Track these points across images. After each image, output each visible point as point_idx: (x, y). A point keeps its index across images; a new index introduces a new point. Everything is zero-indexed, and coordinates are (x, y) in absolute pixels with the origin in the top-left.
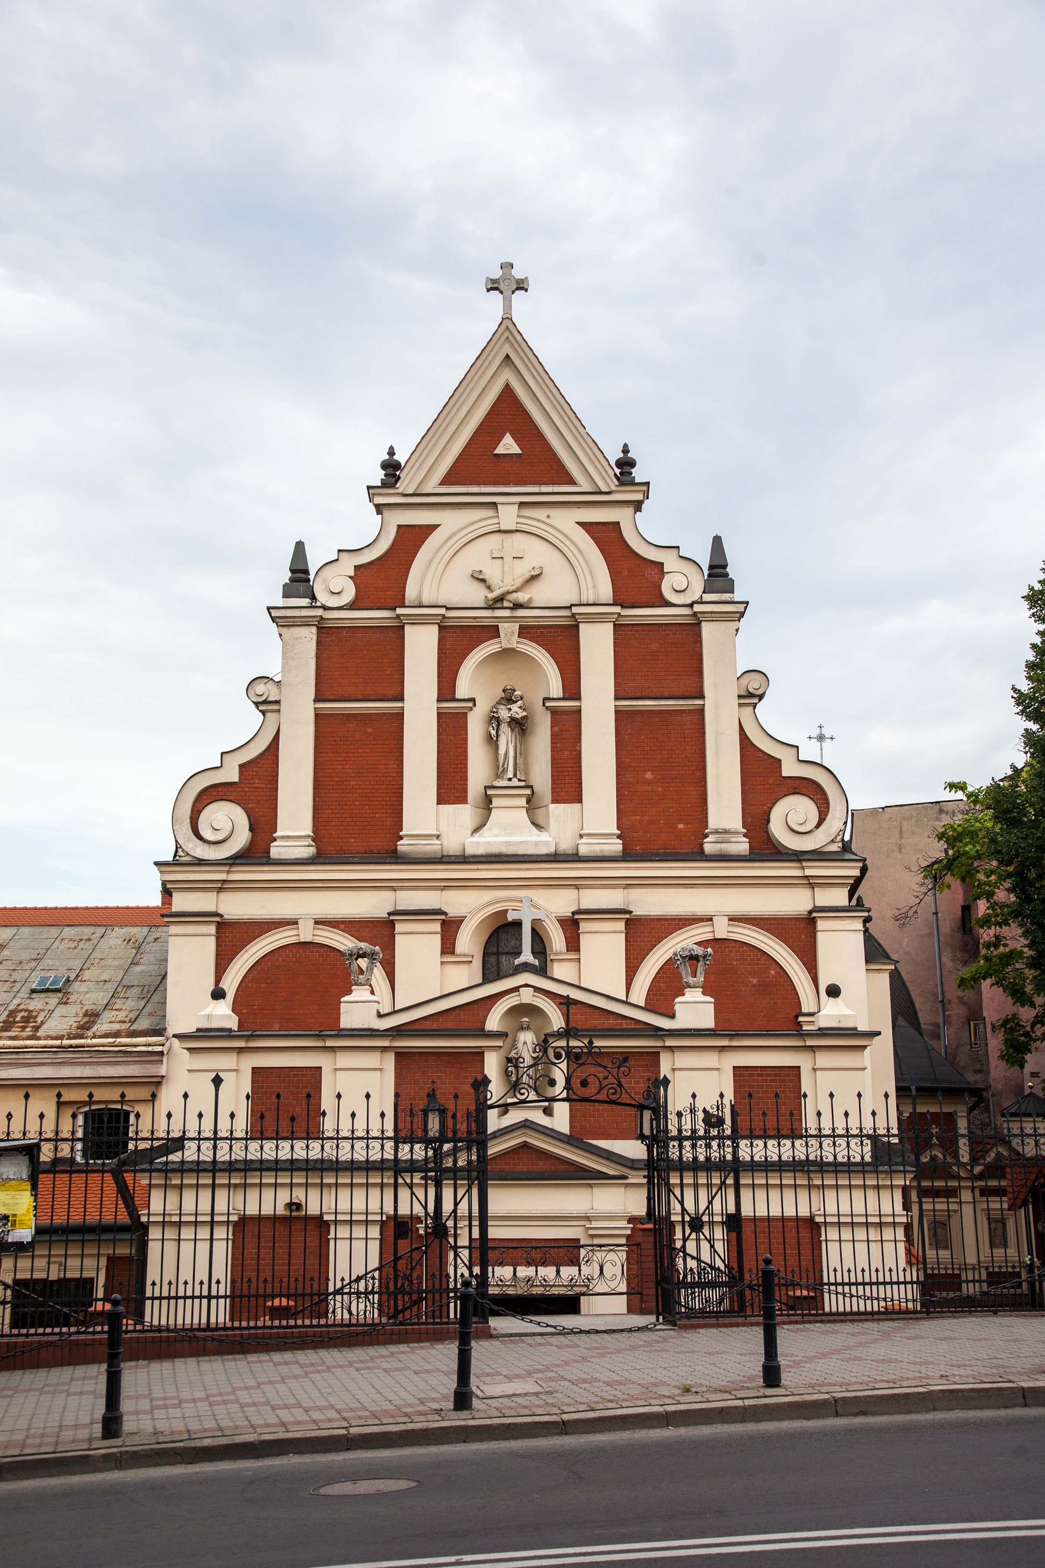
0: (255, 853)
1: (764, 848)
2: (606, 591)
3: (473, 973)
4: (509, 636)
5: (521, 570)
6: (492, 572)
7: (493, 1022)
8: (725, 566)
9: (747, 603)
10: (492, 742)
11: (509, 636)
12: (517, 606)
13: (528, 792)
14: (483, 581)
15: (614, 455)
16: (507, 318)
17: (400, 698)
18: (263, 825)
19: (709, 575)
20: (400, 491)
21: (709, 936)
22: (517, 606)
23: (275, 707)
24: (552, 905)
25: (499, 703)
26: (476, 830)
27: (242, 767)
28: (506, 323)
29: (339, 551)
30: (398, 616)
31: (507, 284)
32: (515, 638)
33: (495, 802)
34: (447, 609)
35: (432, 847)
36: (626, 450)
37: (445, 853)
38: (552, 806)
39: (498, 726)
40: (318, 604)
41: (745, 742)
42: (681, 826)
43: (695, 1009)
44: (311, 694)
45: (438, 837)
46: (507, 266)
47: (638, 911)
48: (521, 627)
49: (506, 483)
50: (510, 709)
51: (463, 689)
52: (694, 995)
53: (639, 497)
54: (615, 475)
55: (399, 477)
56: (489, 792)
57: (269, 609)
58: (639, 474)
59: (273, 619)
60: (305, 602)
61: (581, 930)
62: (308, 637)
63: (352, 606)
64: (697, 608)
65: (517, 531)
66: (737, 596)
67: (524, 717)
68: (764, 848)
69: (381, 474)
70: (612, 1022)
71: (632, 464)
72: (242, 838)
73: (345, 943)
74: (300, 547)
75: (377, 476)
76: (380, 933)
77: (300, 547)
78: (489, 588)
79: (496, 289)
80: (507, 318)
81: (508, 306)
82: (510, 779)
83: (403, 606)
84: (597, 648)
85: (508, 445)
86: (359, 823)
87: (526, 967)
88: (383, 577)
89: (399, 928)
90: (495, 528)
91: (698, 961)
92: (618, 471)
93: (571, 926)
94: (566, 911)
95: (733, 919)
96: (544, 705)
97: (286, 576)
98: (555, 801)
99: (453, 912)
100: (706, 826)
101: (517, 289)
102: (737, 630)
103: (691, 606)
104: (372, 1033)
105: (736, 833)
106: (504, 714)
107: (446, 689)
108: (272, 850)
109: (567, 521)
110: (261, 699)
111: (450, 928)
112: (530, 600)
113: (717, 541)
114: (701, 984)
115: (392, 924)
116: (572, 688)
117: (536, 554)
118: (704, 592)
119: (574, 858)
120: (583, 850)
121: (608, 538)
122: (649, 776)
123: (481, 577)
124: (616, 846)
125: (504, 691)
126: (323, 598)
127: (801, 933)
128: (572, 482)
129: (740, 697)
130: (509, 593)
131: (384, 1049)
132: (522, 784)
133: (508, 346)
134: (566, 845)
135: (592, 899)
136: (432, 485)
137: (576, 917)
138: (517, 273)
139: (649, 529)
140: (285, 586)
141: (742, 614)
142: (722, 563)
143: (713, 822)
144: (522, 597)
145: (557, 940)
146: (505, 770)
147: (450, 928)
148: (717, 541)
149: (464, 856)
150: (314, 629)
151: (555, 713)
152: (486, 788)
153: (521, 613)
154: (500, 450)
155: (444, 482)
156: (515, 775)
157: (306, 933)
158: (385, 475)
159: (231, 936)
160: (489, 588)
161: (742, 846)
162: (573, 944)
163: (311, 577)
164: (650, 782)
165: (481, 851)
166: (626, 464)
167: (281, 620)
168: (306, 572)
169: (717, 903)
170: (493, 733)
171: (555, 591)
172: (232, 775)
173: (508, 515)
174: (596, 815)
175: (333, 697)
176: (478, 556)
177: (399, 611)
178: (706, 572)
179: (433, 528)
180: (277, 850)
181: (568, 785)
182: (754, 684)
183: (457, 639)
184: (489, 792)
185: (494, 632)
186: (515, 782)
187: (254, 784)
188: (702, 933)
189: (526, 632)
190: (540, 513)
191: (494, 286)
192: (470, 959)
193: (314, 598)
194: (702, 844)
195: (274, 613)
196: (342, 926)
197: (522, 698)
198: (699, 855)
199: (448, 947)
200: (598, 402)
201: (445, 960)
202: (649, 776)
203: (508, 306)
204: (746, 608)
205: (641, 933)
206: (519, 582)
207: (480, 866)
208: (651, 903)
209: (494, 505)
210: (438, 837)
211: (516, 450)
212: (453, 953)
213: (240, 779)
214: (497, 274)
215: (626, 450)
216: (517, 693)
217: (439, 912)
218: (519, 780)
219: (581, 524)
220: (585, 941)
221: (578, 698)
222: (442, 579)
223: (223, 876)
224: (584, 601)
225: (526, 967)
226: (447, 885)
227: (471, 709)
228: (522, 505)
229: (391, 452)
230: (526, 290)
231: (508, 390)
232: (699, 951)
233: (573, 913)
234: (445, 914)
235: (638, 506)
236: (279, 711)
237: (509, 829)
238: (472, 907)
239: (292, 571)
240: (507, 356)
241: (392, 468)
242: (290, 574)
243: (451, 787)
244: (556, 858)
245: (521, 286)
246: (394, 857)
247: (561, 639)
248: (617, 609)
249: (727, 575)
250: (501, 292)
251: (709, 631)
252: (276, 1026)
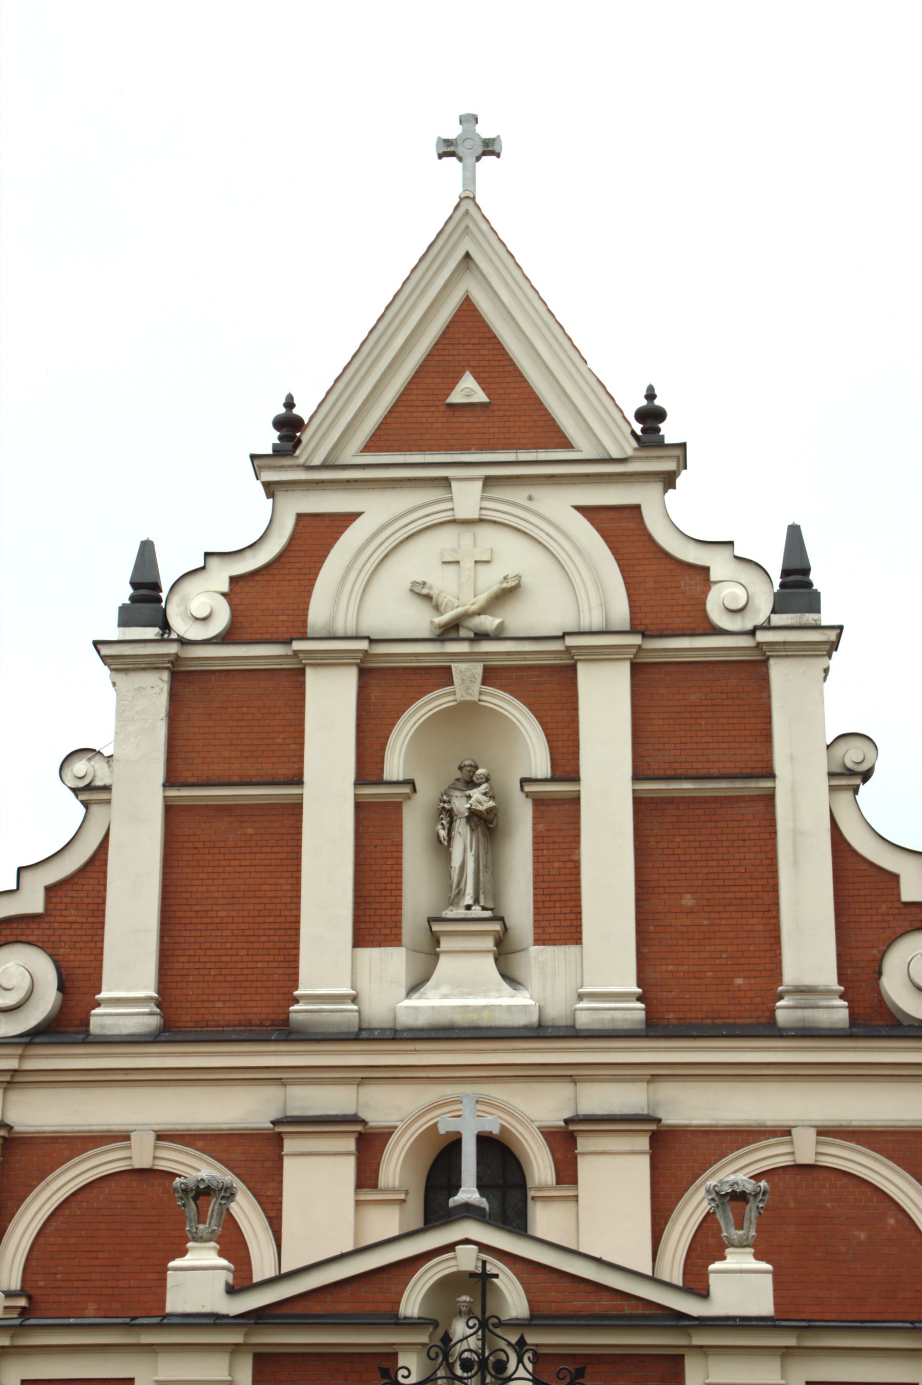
0: (67, 1025)
1: (872, 1017)
2: (620, 609)
3: (386, 1222)
4: (467, 679)
5: (490, 581)
6: (443, 583)
7: (412, 1304)
8: (806, 571)
9: (841, 628)
10: (442, 848)
11: (467, 679)
12: (481, 636)
13: (497, 927)
14: (428, 597)
15: (632, 402)
16: (468, 197)
17: (297, 780)
18: (79, 982)
19: (782, 586)
20: (301, 461)
21: (786, 1161)
22: (481, 636)
23: (103, 796)
24: (530, 1112)
25: (453, 787)
26: (414, 988)
27: (49, 889)
28: (467, 204)
29: (207, 555)
30: (296, 653)
31: (469, 147)
32: (477, 686)
33: (445, 944)
34: (372, 641)
36: (651, 395)
37: (365, 1025)
38: (534, 950)
39: (451, 823)
40: (174, 636)
41: (840, 845)
42: (739, 981)
43: (743, 1284)
44: (158, 773)
45: (354, 999)
46: (469, 120)
47: (672, 1118)
48: (486, 669)
49: (464, 448)
50: (469, 797)
51: (395, 766)
52: (739, 1260)
53: (670, 466)
54: (633, 433)
55: (299, 441)
56: (436, 927)
57: (96, 643)
58: (669, 431)
59: (104, 658)
60: (152, 633)
61: (580, 1149)
62: (155, 690)
63: (225, 638)
64: (762, 636)
65: (481, 521)
66: (827, 617)
67: (490, 810)
69: (274, 436)
70: (605, 1304)
71: (659, 415)
73: (201, 1169)
74: (147, 551)
75: (267, 439)
76: (258, 1158)
77: (147, 551)
78: (437, 608)
79: (452, 154)
80: (468, 197)
81: (470, 179)
82: (468, 907)
83: (304, 638)
85: (468, 390)
86: (228, 978)
87: (468, 1212)
88: (272, 593)
89: (289, 1145)
90: (447, 516)
91: (747, 1202)
92: (638, 427)
93: (564, 1142)
94: (555, 1117)
95: (825, 1132)
96: (522, 787)
97: (125, 593)
98: (539, 941)
99: (376, 1118)
100: (780, 981)
101: (485, 153)
102: (826, 671)
103: (752, 632)
104: (216, 1321)
105: (828, 992)
106: (460, 805)
107: (368, 766)
108: (93, 1021)
109: (559, 507)
110: (81, 784)
112: (501, 627)
113: (794, 534)
114: (751, 1241)
115: (278, 1139)
116: (566, 765)
117: (511, 557)
118: (774, 611)
119: (571, 1033)
120: (584, 1020)
121: (622, 529)
122: (688, 901)
123: (425, 591)
124: (635, 1012)
125: (460, 768)
126: (180, 626)
128: (567, 445)
129: (831, 775)
130: (467, 615)
131: (234, 1349)
132: (488, 914)
133: (464, 241)
134: (557, 1012)
135: (601, 1098)
136: (350, 455)
137: (572, 1127)
138: (484, 131)
139: (685, 515)
140: (123, 609)
141: (834, 646)
142: (805, 567)
143: (792, 974)
144: (489, 622)
145: (540, 1166)
146: (460, 893)
147: (370, 1145)
148: (794, 534)
149: (395, 1031)
150: (166, 675)
151: (539, 802)
152: (431, 920)
153: (486, 647)
154: (456, 397)
155: (371, 446)
156: (477, 901)
158: (280, 438)
160: (437, 608)
161: (837, 1013)
162: (567, 1173)
163: (164, 595)
164: (690, 911)
165: (421, 1021)
166: (651, 416)
167: (118, 661)
168: (157, 587)
170: (443, 833)
172: (33, 902)
173: (467, 498)
174: (605, 964)
175: (194, 780)
176: (421, 562)
177: (297, 645)
178: (777, 580)
179: (352, 517)
180: (102, 1020)
181: (560, 917)
182: (852, 755)
184: (436, 927)
185: (442, 676)
186: (477, 912)
187: (67, 917)
188: (772, 1155)
189: (493, 676)
190: (519, 495)
191: (448, 149)
192: (402, 1196)
193: (165, 626)
194: (773, 1011)
195: (105, 651)
196: (200, 1144)
197: (487, 779)
198: (769, 1029)
199: (366, 1177)
200: (608, 325)
201: (362, 1197)
202: (688, 901)
203: (470, 179)
204: (839, 636)
205: (675, 1156)
206: (482, 599)
207: (420, 1046)
208: (693, 1106)
209: (446, 482)
210: (354, 999)
211: (480, 397)
212: (374, 1186)
213: (46, 908)
214: (453, 131)
215: (651, 395)
216: (481, 771)
217: (354, 1119)
218: (484, 908)
219: (581, 509)
220: (586, 1168)
221: (574, 777)
223: (13, 1064)
224: (585, 627)
225: (468, 1212)
226: (365, 1077)
227: (408, 797)
228: (488, 481)
229: (290, 404)
230: (498, 155)
231: (468, 308)
232: (749, 1186)
233: (567, 1121)
234: (364, 1122)
235: (669, 480)
236: (108, 802)
237: (466, 987)
239: (134, 585)
240: (467, 256)
241: (289, 426)
242: (130, 591)
243: (374, 919)
244: (539, 1032)
245: (490, 148)
246: (284, 1032)
247: (548, 684)
248: (636, 640)
249: (809, 585)
250: (460, 159)
251: (780, 674)
252: (92, 1308)
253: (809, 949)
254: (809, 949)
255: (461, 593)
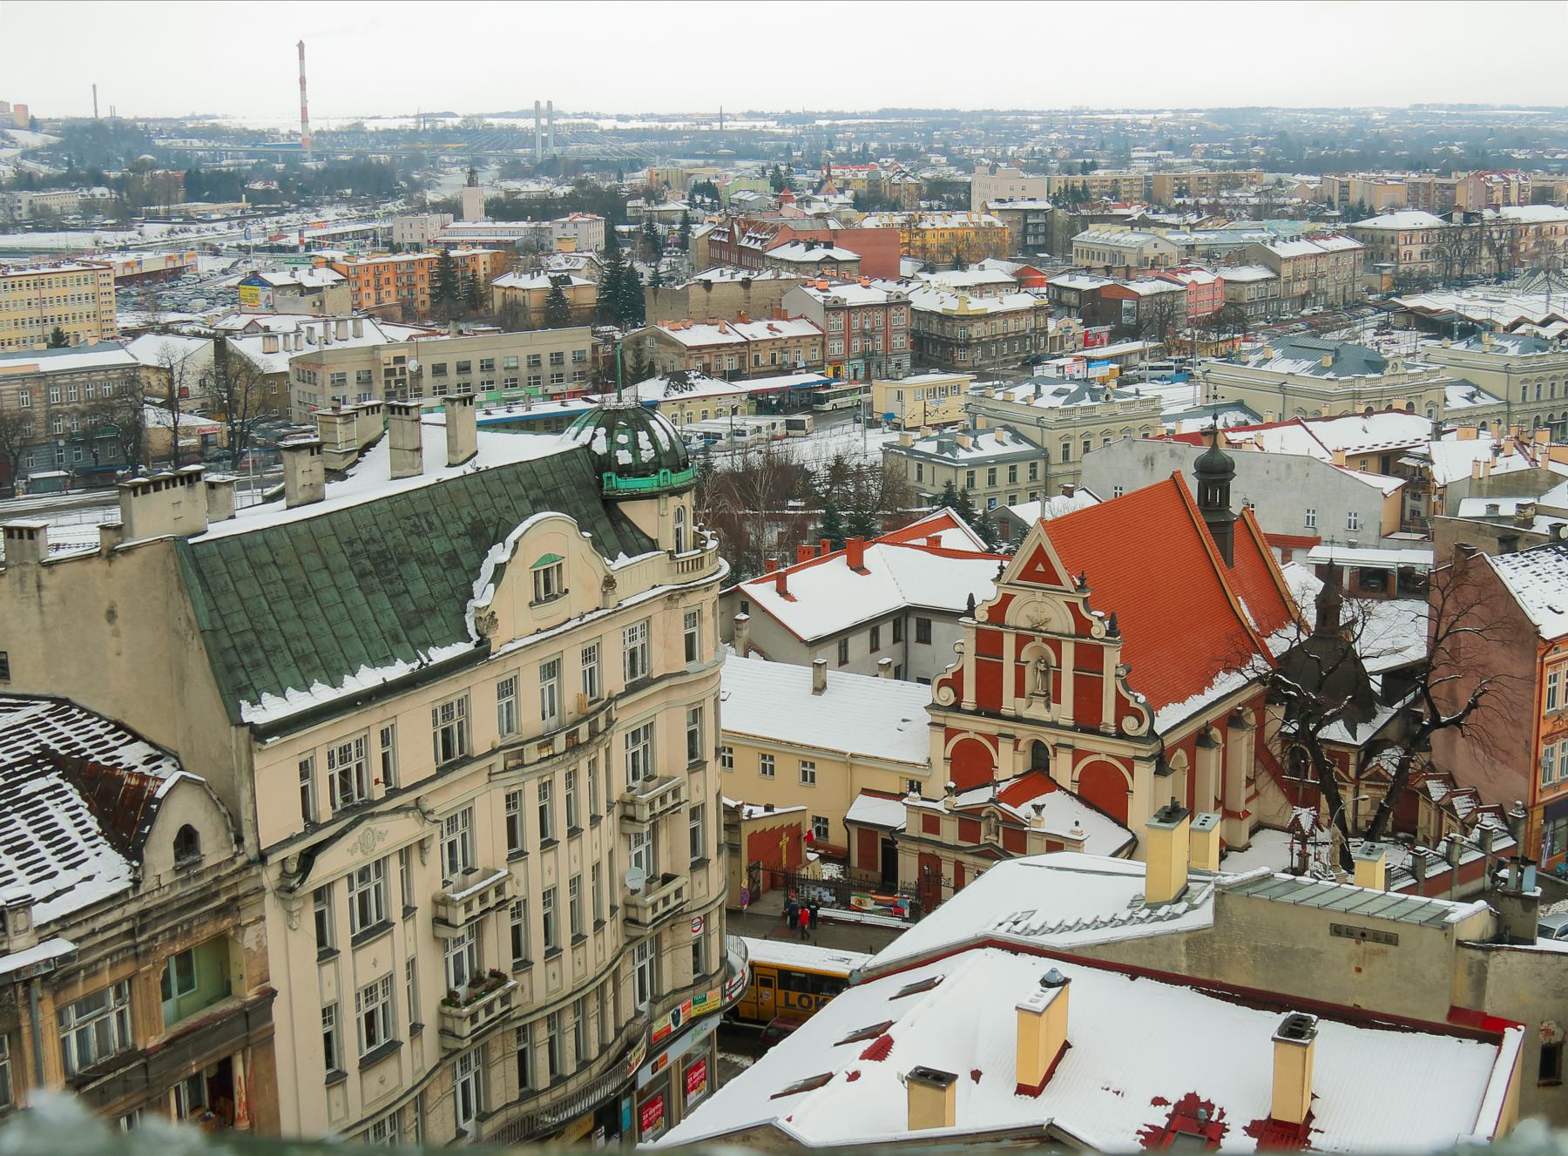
0: (956, 707)
1: (1121, 735)
35: (1012, 713)
68: (1121, 735)
72: (952, 700)
74: (971, 596)
77: (971, 596)
84: (1068, 650)
85: (1040, 568)
86: (989, 705)
88: (998, 612)
107: (1017, 659)
109: (1061, 600)
111: (1017, 742)
116: (1059, 665)
124: (1071, 723)
127: (1129, 763)
157: (972, 735)
159: (950, 733)
161: (1112, 730)
169: (1103, 749)
171: (1055, 626)
174: (1064, 711)
181: (1058, 700)
183: (1022, 641)
185: (1032, 639)
189: (1045, 640)
199: (1016, 749)
208: (1080, 745)
222: (1017, 615)
237: (1037, 711)
238: (1026, 734)
243: (1020, 692)
247: (1056, 646)
253: (1108, 715)
254: (1108, 715)
255: (1037, 617)
